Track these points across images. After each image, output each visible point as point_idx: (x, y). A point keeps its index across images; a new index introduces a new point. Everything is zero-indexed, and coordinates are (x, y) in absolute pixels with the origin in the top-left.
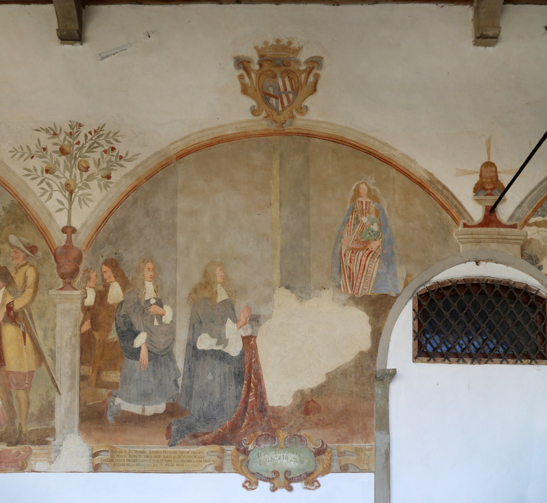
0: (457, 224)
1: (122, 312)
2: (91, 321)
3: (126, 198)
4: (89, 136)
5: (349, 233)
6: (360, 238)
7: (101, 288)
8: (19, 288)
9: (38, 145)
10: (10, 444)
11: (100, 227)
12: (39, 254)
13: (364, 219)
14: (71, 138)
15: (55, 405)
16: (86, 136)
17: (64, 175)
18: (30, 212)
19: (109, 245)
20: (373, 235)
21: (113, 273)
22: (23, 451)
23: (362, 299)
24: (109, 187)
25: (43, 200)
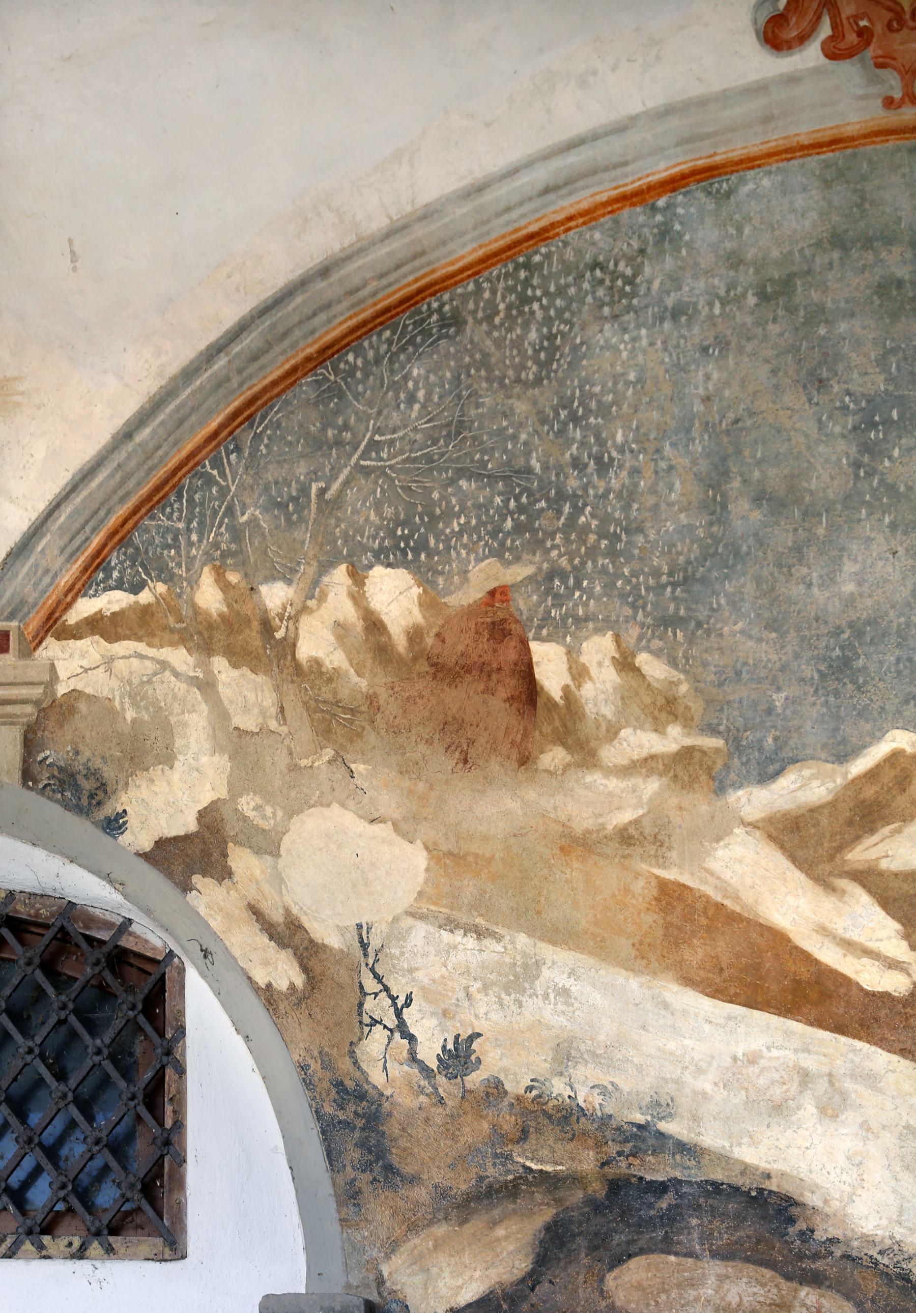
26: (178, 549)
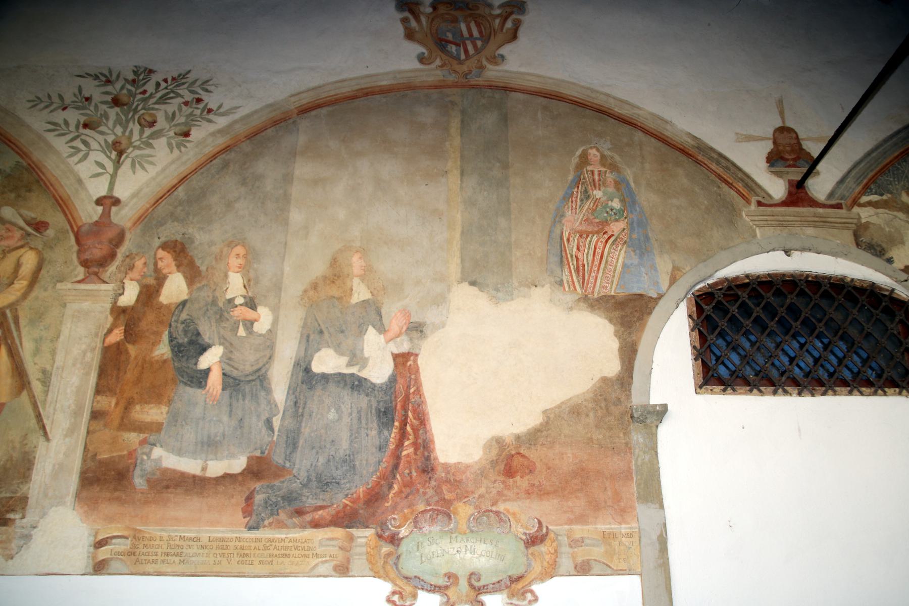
0: (747, 202)
1: (184, 316)
2: (125, 330)
3: (211, 161)
4: (163, 85)
5: (574, 211)
6: (591, 217)
11: (161, 198)
12: (50, 233)
13: (598, 194)
15: (35, 458)
16: (158, 85)
17: (113, 131)
18: (46, 177)
19: (173, 222)
20: (613, 214)
21: (175, 260)
23: (601, 301)
24: (185, 147)
25: (71, 163)
26: (892, 185)
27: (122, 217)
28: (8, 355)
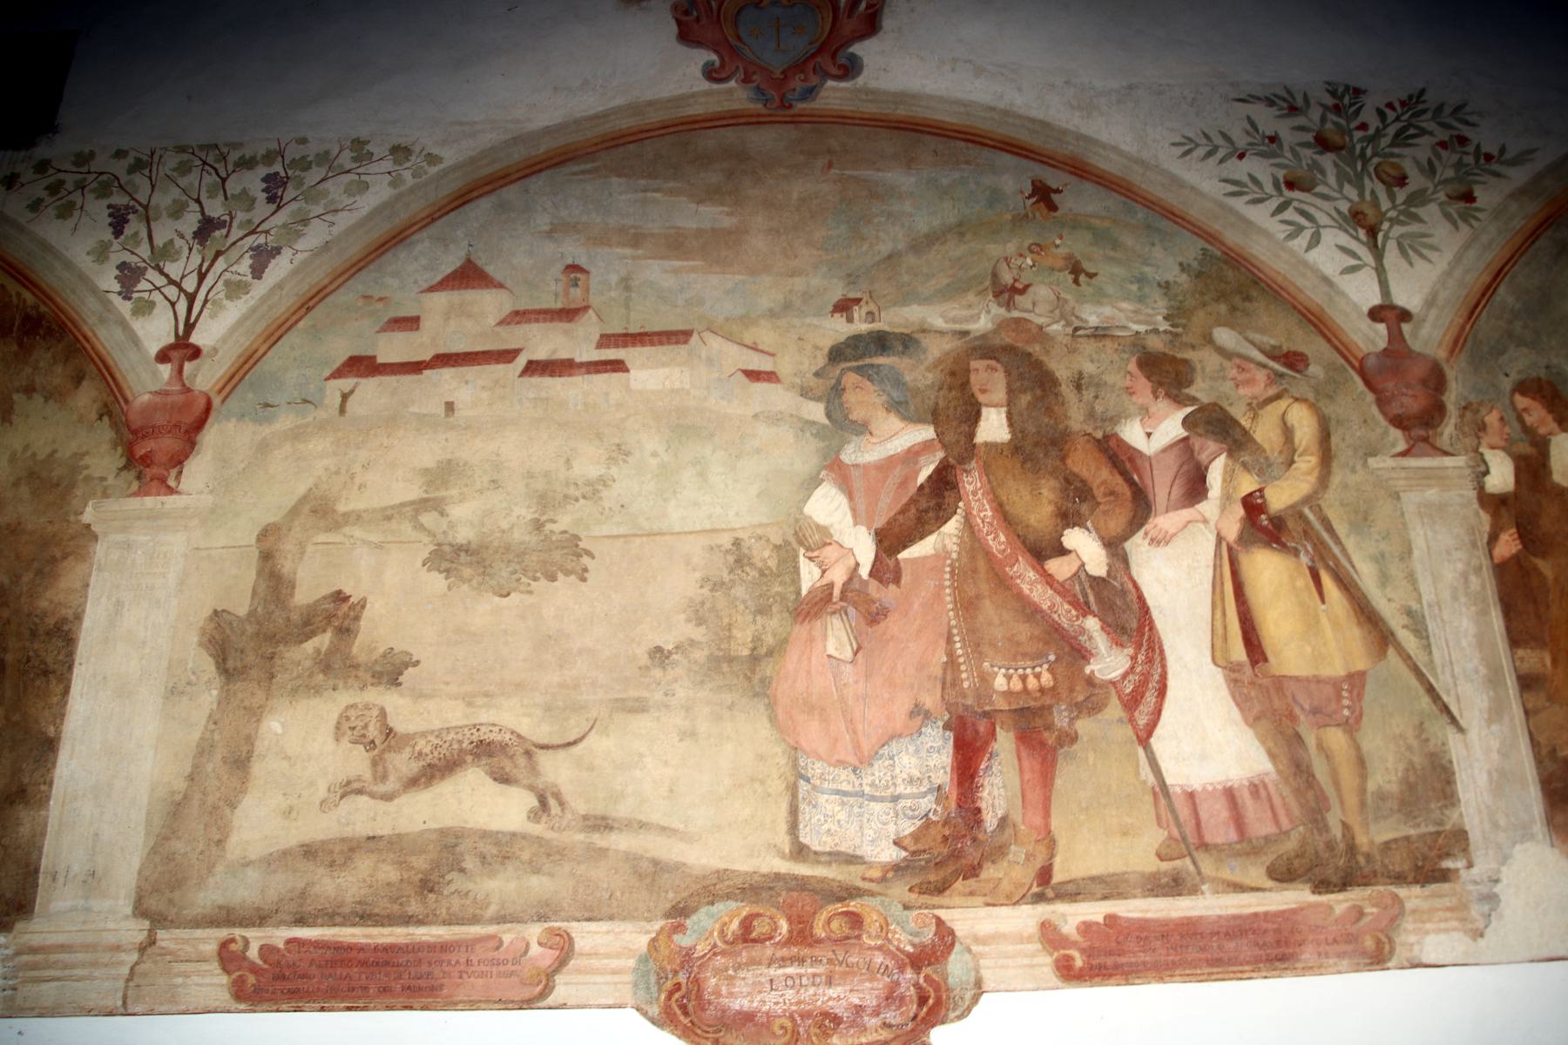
2: (1518, 532)
4: (1391, 115)
7: (1525, 448)
8: (1275, 456)
9: (1252, 130)
10: (1322, 886)
11: (1476, 306)
12: (1314, 369)
14: (1340, 116)
15: (1451, 762)
16: (1381, 114)
19: (1518, 346)
21: (1550, 411)
22: (1373, 906)
24: (1477, 219)
27: (1428, 337)
28: (1339, 588)
